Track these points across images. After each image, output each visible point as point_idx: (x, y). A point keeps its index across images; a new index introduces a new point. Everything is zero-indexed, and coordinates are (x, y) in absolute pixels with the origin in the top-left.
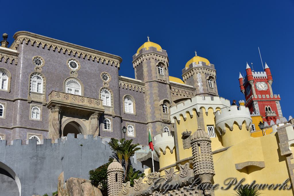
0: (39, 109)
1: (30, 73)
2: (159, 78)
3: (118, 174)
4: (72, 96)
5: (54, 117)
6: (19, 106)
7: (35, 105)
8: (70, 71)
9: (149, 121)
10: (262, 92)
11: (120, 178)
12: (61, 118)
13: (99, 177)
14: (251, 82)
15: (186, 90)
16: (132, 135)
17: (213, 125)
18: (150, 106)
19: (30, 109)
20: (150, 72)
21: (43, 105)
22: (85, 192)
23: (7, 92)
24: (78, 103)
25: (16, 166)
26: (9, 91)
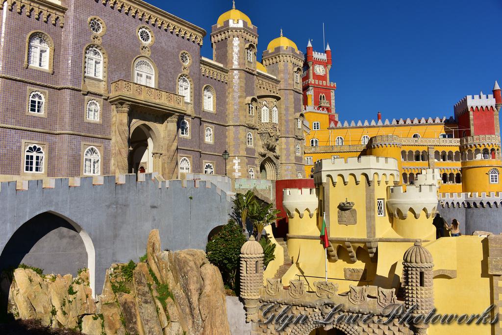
0: (98, 104)
2: (247, 67)
4: (147, 89)
5: (121, 120)
7: (93, 98)
8: (141, 46)
9: (231, 123)
12: (130, 122)
14: (310, 64)
15: (270, 82)
16: (209, 141)
19: (86, 103)
21: (104, 99)
22: (207, 282)
23: (49, 73)
25: (85, 220)
26: (51, 72)
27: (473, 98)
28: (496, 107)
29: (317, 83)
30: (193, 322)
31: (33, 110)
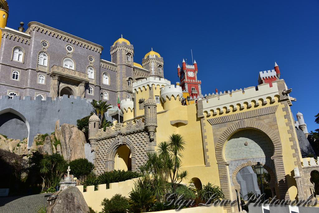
0: (44, 77)
1: (39, 51)
3: (96, 123)
5: (55, 83)
6: (29, 73)
9: (119, 90)
10: (191, 78)
11: (97, 126)
12: (59, 84)
13: (83, 124)
14: (185, 71)
16: (107, 99)
17: (159, 96)
18: (120, 80)
19: (38, 76)
20: (121, 58)
21: (47, 74)
22: (74, 134)
23: (22, 63)
24: (71, 75)
25: (26, 113)
26: (23, 63)
27: (263, 73)
28: (277, 76)
29: (189, 81)
30: (67, 151)
31: (14, 78)
